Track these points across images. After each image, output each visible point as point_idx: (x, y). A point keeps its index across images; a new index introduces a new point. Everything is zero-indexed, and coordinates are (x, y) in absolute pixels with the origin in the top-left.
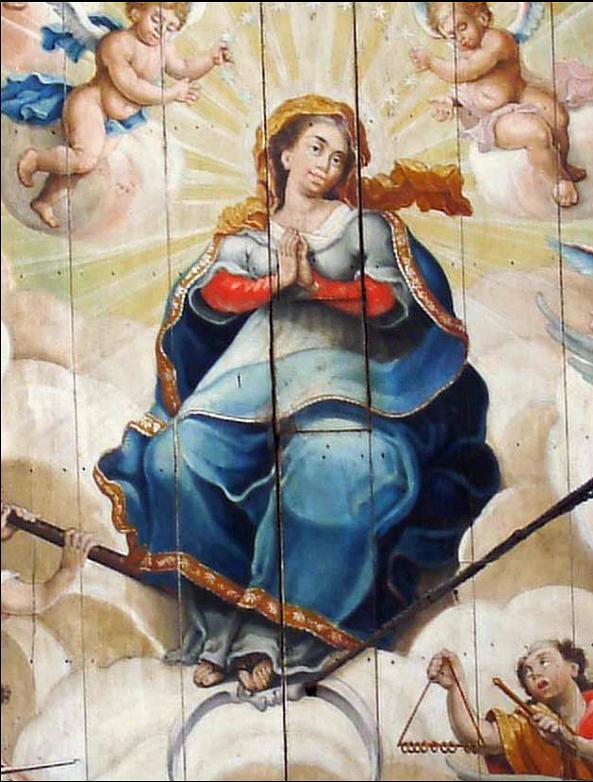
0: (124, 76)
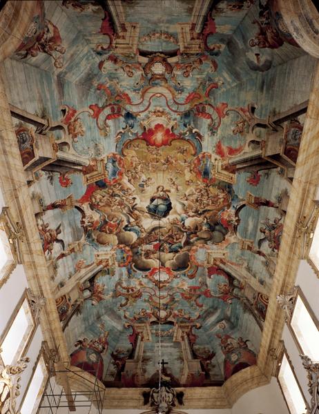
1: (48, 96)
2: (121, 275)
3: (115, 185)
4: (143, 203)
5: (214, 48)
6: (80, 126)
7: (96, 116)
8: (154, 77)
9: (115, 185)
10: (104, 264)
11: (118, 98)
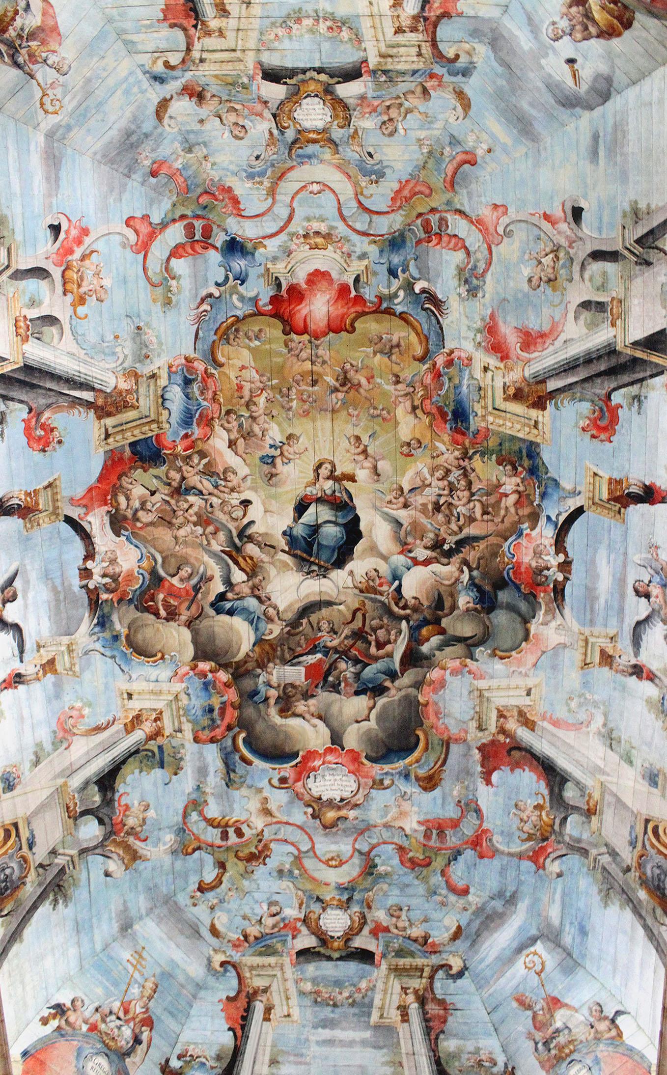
0: (286, 454)
1: (16, 187)
2: (202, 772)
3: (189, 457)
4: (272, 519)
5: (457, 56)
6: (97, 274)
7: (144, 248)
8: (303, 138)
9: (189, 457)
10: (148, 727)
11: (204, 200)
